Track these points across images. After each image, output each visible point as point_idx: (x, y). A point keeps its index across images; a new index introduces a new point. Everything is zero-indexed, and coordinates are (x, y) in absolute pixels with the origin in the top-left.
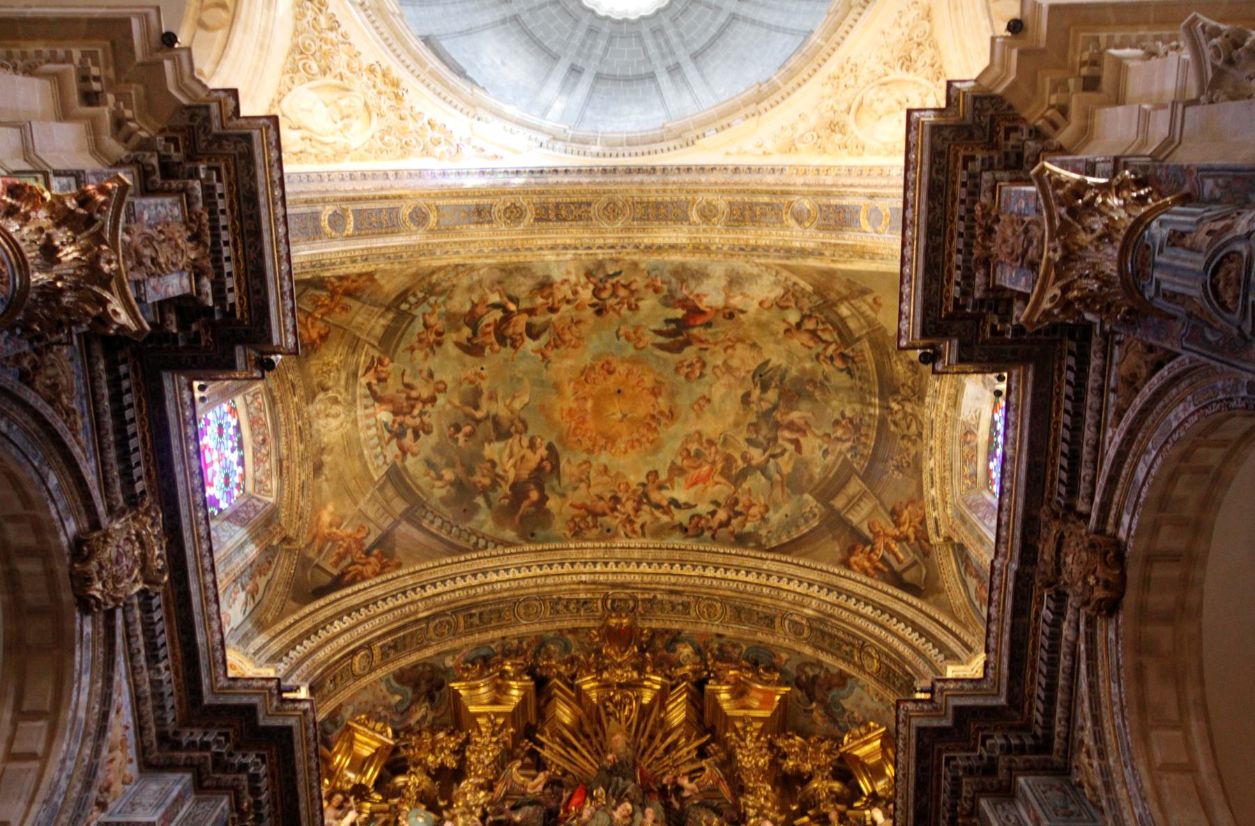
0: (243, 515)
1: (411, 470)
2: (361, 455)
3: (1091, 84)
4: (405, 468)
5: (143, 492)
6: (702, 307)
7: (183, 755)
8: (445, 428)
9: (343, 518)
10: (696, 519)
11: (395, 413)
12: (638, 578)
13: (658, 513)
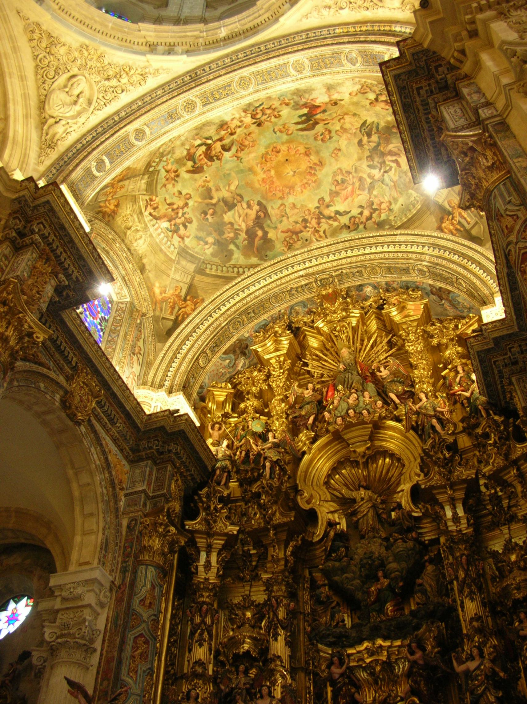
0: (118, 318)
1: (189, 245)
2: (161, 250)
3: (474, 34)
4: (186, 246)
5: (77, 363)
6: (317, 104)
7: (144, 453)
8: (199, 216)
9: (165, 287)
10: (353, 219)
11: (170, 221)
12: (330, 265)
13: (330, 222)
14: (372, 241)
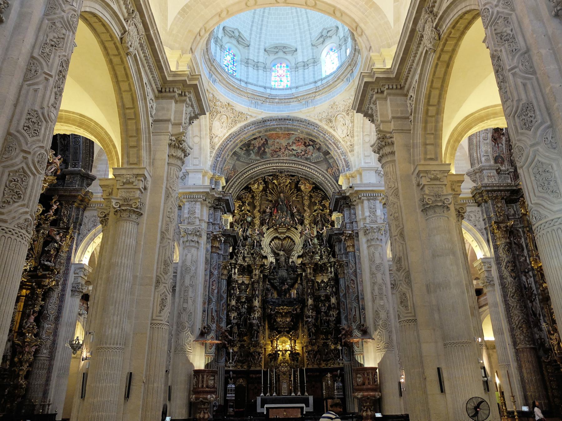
14: (302, 164)
